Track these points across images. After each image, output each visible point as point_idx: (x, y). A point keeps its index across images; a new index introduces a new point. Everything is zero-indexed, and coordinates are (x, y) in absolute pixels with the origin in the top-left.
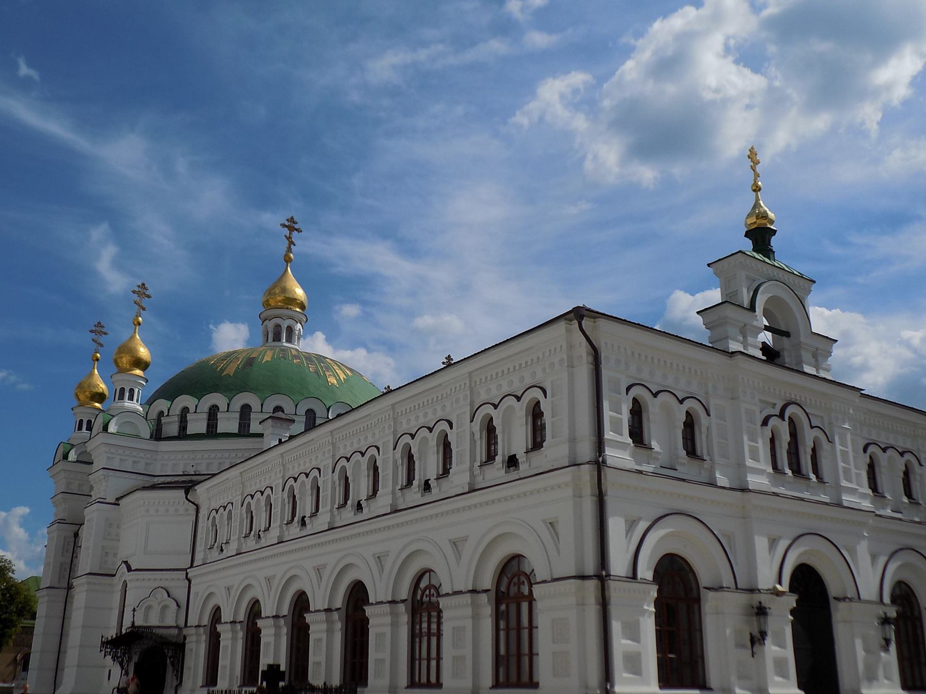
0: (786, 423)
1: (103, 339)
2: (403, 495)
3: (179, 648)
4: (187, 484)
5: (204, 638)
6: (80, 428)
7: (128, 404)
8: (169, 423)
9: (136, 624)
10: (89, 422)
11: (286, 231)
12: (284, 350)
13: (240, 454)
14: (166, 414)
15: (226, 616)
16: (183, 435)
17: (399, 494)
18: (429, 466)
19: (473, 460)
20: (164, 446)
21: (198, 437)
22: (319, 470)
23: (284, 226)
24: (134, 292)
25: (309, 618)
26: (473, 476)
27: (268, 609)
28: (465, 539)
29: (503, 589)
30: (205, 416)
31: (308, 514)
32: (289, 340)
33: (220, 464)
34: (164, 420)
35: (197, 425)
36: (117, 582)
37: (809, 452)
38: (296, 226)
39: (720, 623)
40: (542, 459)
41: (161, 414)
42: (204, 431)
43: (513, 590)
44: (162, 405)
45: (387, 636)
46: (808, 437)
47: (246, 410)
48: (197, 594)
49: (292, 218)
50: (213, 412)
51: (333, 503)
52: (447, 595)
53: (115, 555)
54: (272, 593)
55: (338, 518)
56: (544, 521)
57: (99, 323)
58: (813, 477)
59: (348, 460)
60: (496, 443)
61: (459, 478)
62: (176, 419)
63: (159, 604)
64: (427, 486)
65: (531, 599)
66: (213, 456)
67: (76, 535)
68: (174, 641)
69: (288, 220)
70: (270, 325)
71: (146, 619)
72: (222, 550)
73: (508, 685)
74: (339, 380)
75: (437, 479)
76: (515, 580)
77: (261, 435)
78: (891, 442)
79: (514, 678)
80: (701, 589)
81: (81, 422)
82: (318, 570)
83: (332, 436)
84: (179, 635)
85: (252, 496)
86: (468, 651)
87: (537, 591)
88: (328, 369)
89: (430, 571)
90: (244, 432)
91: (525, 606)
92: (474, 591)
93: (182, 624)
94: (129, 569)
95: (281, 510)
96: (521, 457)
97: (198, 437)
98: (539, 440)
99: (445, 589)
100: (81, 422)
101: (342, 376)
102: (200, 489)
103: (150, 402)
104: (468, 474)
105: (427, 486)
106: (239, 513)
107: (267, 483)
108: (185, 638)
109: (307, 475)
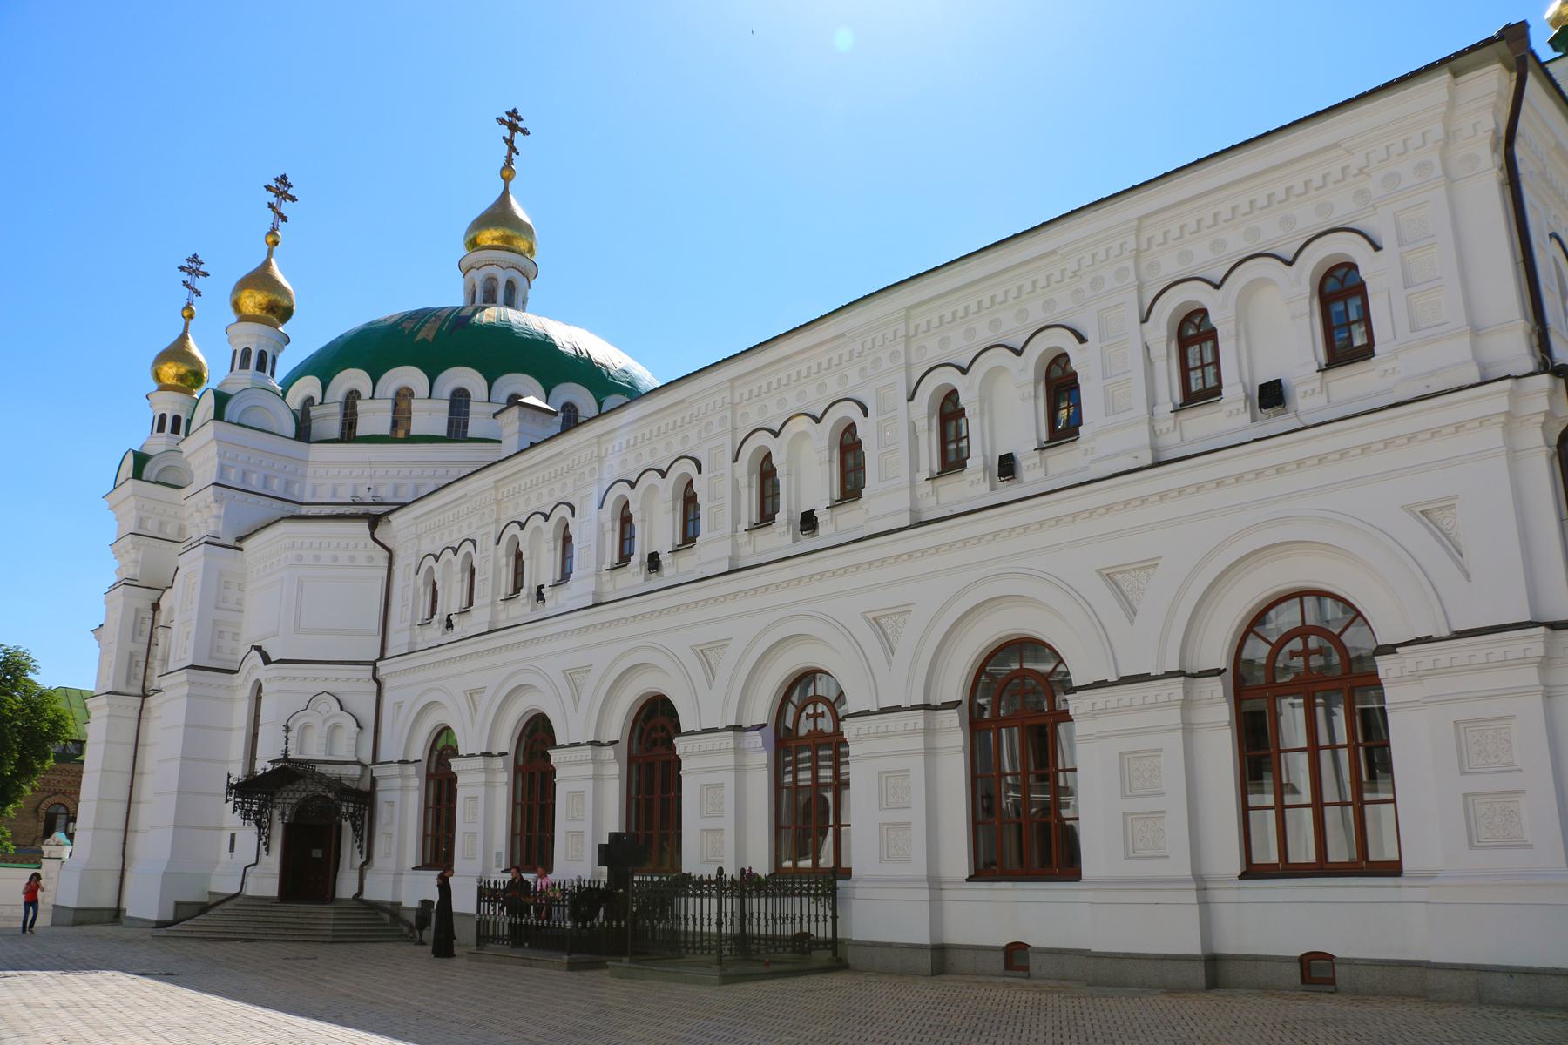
1: (199, 283)
2: (935, 491)
3: (362, 800)
6: (161, 429)
8: (324, 416)
9: (293, 755)
10: (177, 419)
11: (506, 132)
14: (318, 399)
16: (348, 434)
20: (317, 452)
23: (502, 121)
24: (268, 188)
30: (389, 405)
32: (509, 303)
33: (417, 488)
34: (314, 411)
35: (375, 417)
36: (242, 687)
38: (521, 125)
41: (309, 401)
42: (385, 429)
47: (460, 400)
48: (399, 705)
49: (515, 111)
50: (403, 398)
56: (1408, 509)
57: (195, 256)
63: (324, 722)
66: (406, 471)
67: (156, 607)
69: (508, 114)
70: (478, 277)
72: (449, 625)
76: (1296, 644)
83: (732, 388)
84: (362, 776)
90: (457, 431)
93: (366, 757)
94: (267, 660)
99: (852, 705)
100: (163, 418)
102: (398, 520)
104: (1145, 428)
108: (374, 780)
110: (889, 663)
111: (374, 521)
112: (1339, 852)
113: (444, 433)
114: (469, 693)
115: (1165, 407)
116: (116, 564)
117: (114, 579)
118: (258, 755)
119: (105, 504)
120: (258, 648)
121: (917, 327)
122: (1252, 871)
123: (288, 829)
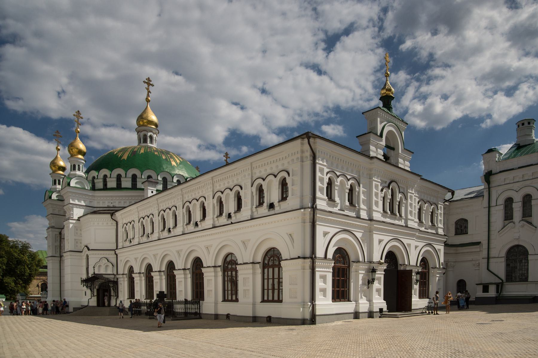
0: (390, 191)
2: (218, 220)
4: (112, 211)
5: (126, 279)
7: (78, 173)
12: (151, 147)
13: (137, 198)
15: (136, 270)
17: (216, 219)
18: (230, 206)
19: (252, 205)
21: (112, 189)
22: (176, 207)
25: (175, 272)
26: (252, 212)
27: (155, 268)
28: (249, 240)
29: (266, 262)
31: (171, 227)
37: (398, 203)
39: (358, 275)
40: (285, 205)
43: (271, 263)
44: (94, 173)
45: (213, 282)
46: (399, 196)
51: (184, 222)
52: (241, 264)
54: (157, 262)
55: (186, 229)
58: (398, 214)
59: (190, 203)
60: (263, 197)
61: (246, 212)
62: (101, 180)
64: (229, 216)
65: (279, 266)
68: (113, 280)
71: (99, 270)
73: (268, 301)
74: (177, 163)
75: (235, 213)
76: (272, 259)
77: (143, 189)
78: (428, 199)
79: (270, 298)
80: (351, 262)
82: (178, 252)
85: (144, 218)
86: (251, 288)
87: (282, 263)
88: (172, 157)
89: (232, 254)
91: (276, 270)
92: (253, 263)
95: (158, 225)
96: (276, 204)
97: (112, 189)
98: (285, 196)
101: (178, 161)
102: (117, 214)
103: (87, 172)
104: (250, 211)
105: (229, 216)
106: (137, 226)
107: (150, 212)
109: (170, 209)
111: (112, 214)
112: (276, 298)
113: (130, 187)
115: (255, 206)
122: (263, 301)
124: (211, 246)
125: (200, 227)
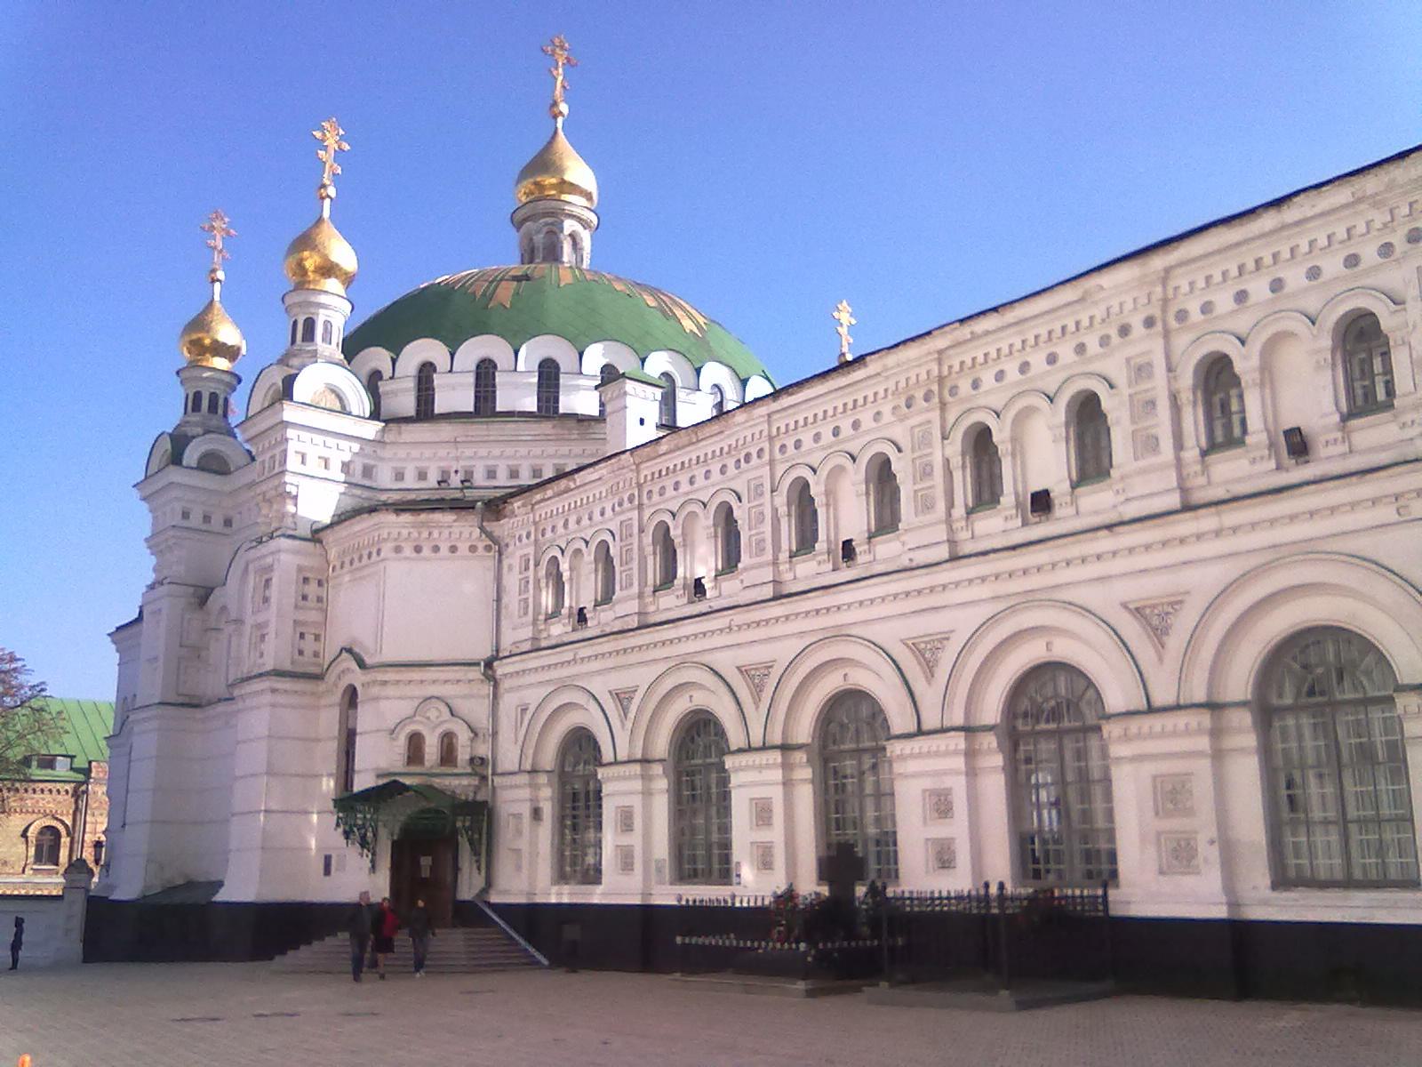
2: (1205, 469)
6: (196, 407)
8: (395, 393)
10: (214, 397)
16: (425, 411)
30: (471, 379)
35: (455, 394)
42: (471, 409)
53: (317, 637)
81: (198, 396)
83: (940, 362)
94: (362, 664)
100: (198, 396)
110: (1161, 659)
114: (622, 692)
116: (153, 560)
117: (150, 577)
118: (358, 764)
119: (136, 493)
120: (350, 651)
121: (1176, 289)
123: (397, 848)
124: (1176, 603)
125: (1063, 518)
